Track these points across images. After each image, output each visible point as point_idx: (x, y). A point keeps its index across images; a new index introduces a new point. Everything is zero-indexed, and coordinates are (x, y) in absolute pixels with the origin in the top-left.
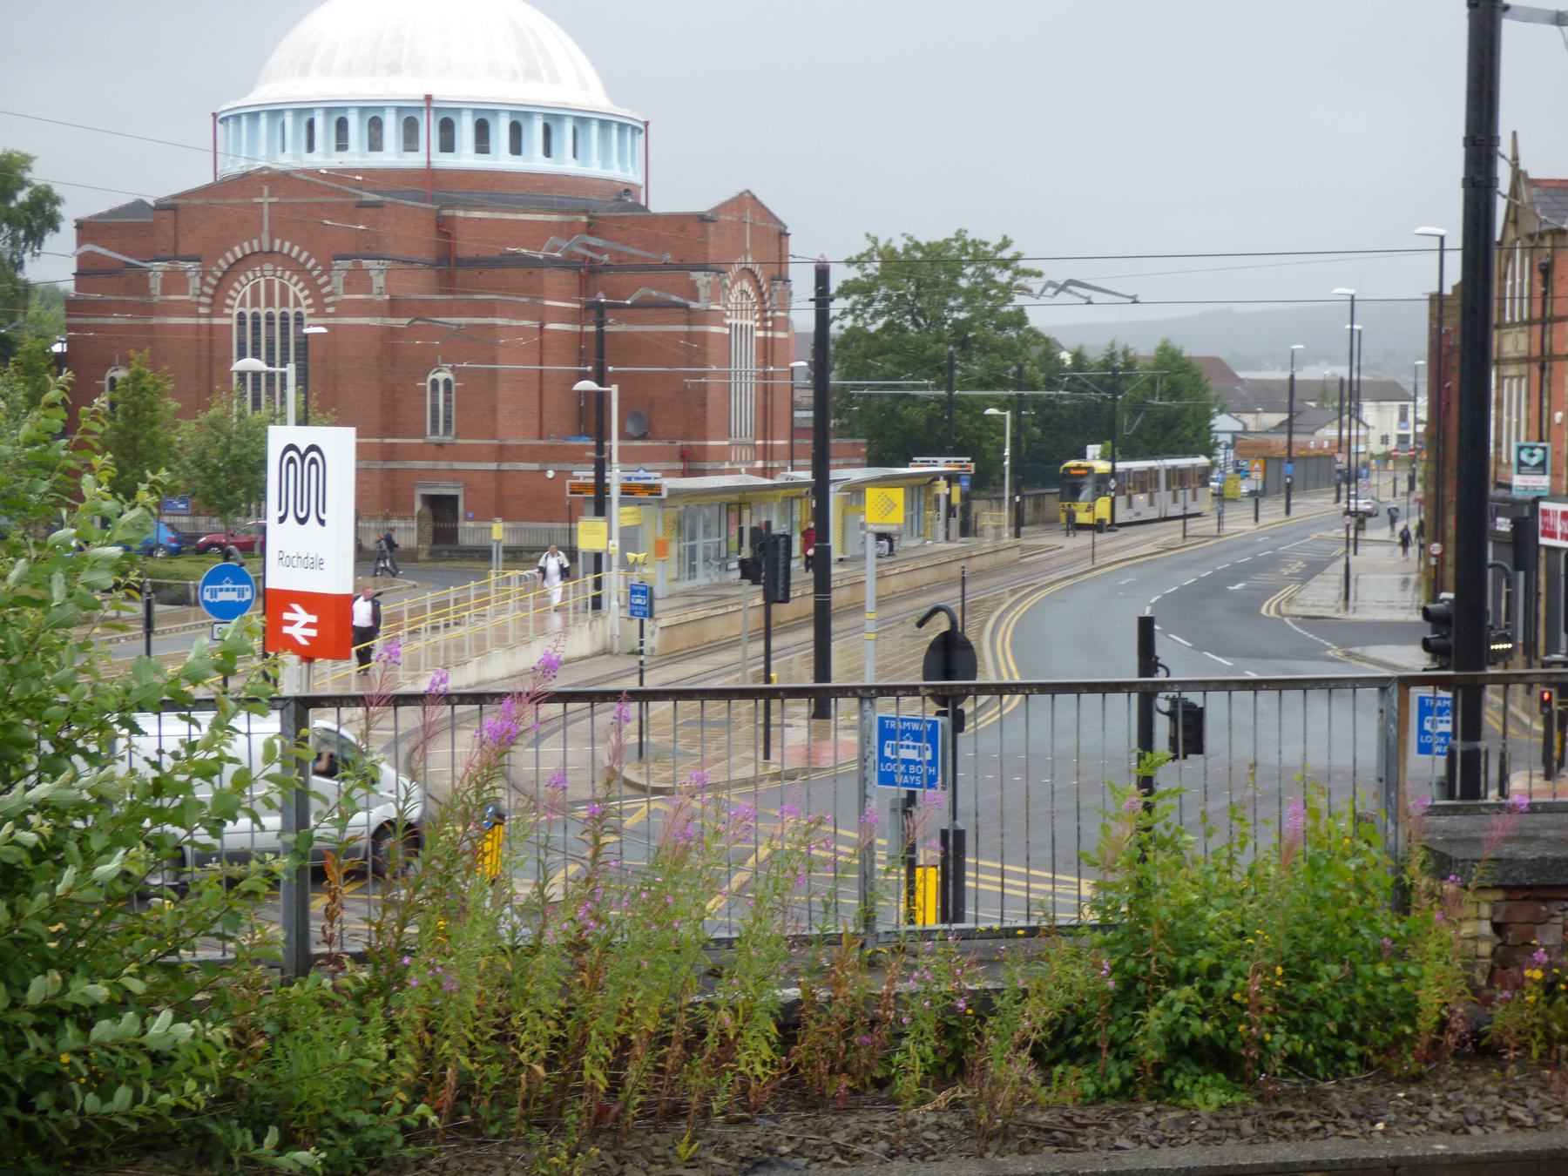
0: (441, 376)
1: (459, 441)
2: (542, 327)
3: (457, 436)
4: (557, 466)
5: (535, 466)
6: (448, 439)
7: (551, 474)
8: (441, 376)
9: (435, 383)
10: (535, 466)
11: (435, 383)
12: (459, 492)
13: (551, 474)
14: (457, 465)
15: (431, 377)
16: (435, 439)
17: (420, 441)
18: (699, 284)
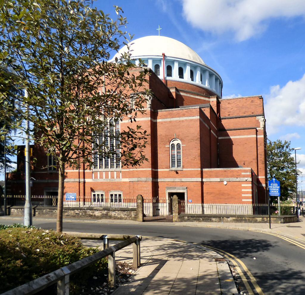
0: (176, 143)
1: (184, 169)
2: (210, 130)
3: (183, 167)
4: (228, 179)
5: (218, 180)
6: (179, 169)
7: (225, 183)
8: (176, 143)
9: (173, 146)
10: (218, 180)
11: (173, 146)
12: (185, 191)
13: (225, 183)
14: (184, 180)
15: (171, 143)
16: (174, 169)
17: (168, 170)
18: (260, 121)
